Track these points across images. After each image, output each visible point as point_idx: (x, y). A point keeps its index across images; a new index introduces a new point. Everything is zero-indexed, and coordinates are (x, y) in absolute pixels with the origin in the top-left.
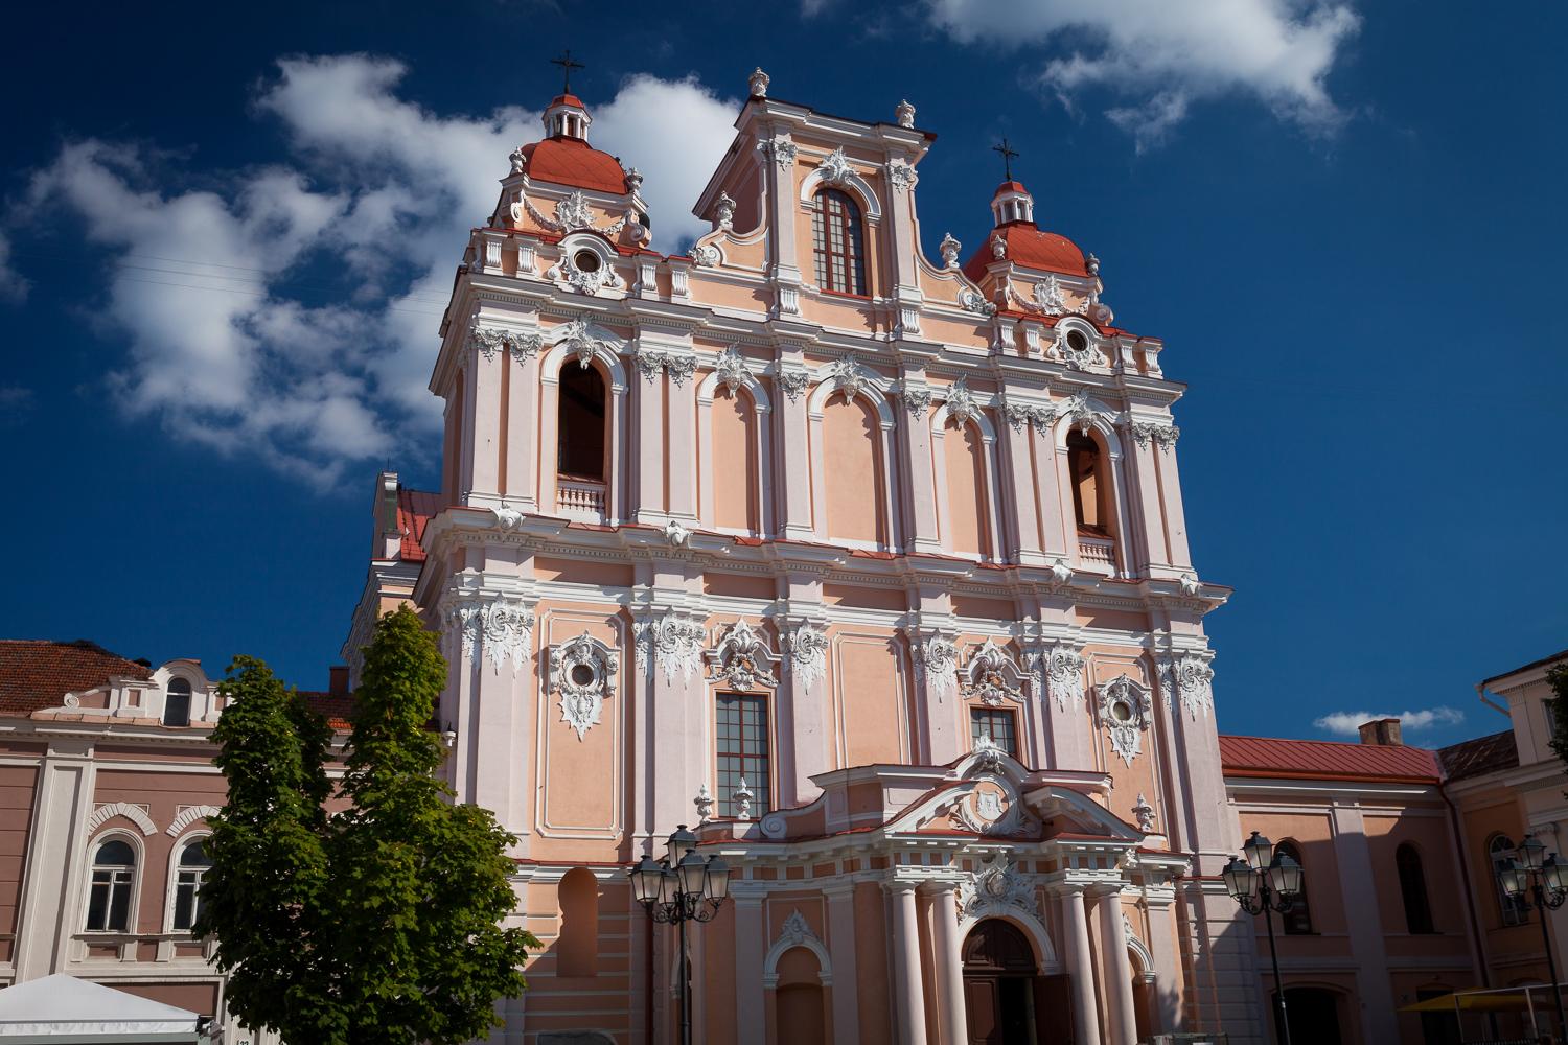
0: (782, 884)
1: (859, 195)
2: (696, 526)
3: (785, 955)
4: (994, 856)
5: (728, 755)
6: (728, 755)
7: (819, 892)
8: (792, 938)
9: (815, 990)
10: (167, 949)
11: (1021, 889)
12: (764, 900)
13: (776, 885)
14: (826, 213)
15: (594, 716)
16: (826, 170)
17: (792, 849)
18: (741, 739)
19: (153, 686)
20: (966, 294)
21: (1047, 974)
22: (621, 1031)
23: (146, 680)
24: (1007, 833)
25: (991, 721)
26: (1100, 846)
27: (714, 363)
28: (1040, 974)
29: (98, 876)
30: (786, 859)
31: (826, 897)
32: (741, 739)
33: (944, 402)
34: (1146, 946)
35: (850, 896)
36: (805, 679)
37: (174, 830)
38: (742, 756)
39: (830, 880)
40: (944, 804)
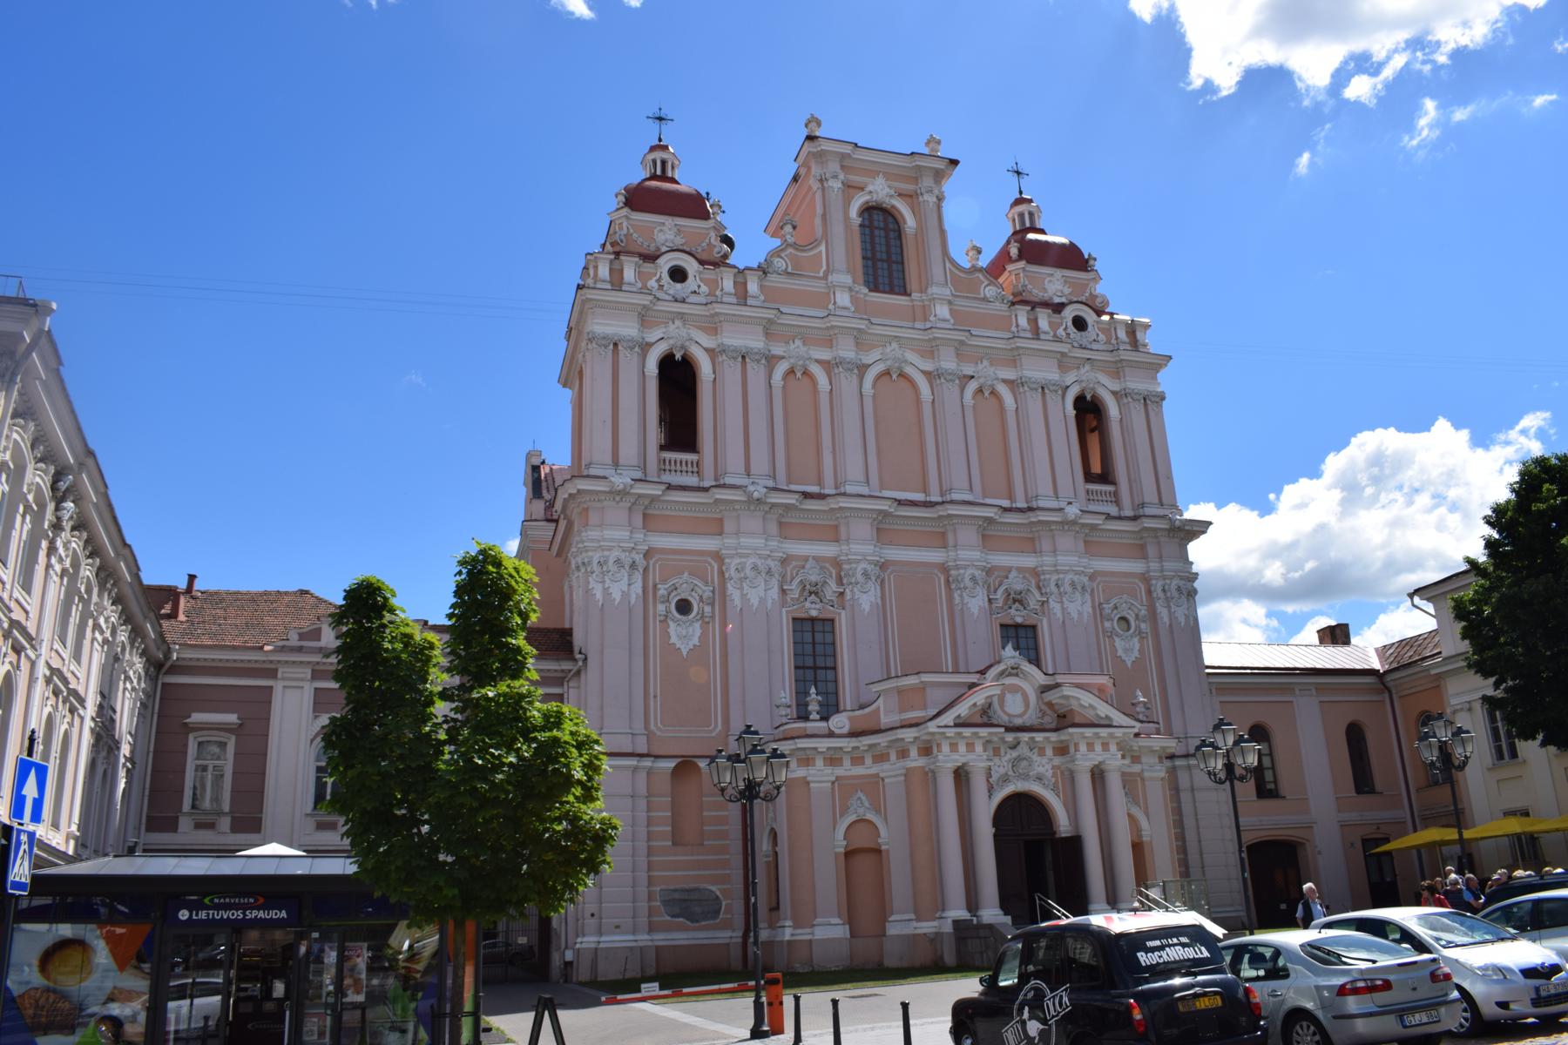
0: (847, 769)
1: (897, 210)
2: (771, 484)
3: (854, 823)
4: (1019, 743)
5: (804, 668)
6: (804, 668)
7: (877, 775)
11: (1041, 769)
12: (833, 783)
14: (871, 227)
15: (696, 641)
16: (871, 192)
17: (854, 742)
20: (987, 289)
21: (1063, 835)
22: (725, 887)
26: (1104, 732)
28: (1057, 836)
30: (850, 749)
31: (883, 779)
32: (814, 655)
33: (973, 377)
35: (903, 778)
38: (815, 668)
39: (886, 766)
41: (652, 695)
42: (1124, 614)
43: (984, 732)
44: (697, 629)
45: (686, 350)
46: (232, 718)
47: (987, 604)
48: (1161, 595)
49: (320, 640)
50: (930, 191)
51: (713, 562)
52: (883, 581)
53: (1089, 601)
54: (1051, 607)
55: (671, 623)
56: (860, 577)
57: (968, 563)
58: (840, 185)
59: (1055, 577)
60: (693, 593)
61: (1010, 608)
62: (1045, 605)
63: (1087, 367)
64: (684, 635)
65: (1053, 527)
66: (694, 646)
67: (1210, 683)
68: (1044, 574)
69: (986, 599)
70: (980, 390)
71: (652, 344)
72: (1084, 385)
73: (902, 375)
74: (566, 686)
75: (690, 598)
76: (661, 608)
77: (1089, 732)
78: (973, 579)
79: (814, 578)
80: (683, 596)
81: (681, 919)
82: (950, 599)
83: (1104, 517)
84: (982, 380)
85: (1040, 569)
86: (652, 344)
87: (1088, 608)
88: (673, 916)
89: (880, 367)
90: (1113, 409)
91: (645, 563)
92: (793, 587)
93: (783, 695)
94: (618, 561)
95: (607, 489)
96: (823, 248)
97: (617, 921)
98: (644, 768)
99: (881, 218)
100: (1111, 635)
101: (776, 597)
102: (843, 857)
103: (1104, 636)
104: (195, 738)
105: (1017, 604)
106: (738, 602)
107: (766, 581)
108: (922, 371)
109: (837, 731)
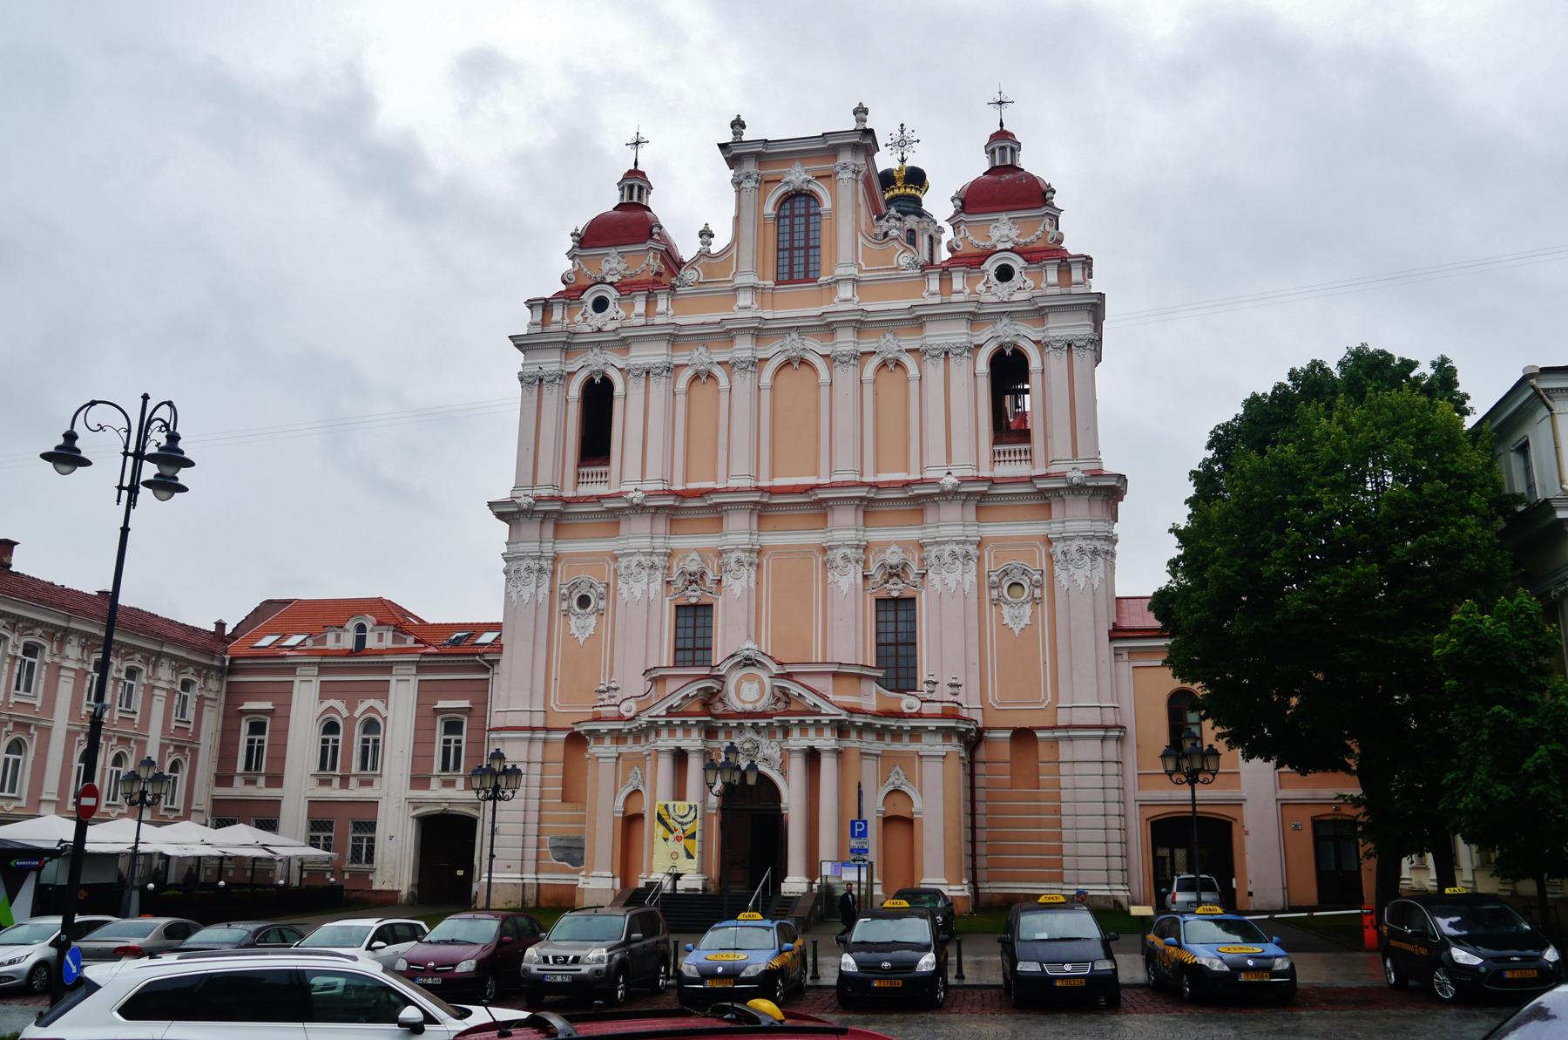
6: (685, 649)
9: (640, 817)
10: (353, 782)
15: (591, 631)
18: (694, 638)
19: (345, 631)
20: (903, 255)
23: (342, 627)
24: (760, 711)
26: (810, 719)
27: (689, 360)
29: (325, 741)
33: (875, 353)
37: (357, 714)
41: (553, 678)
43: (692, 721)
44: (593, 620)
45: (604, 373)
46: (268, 705)
47: (860, 580)
48: (1061, 557)
49: (325, 644)
50: (845, 167)
51: (610, 562)
52: (758, 566)
53: (974, 569)
55: (572, 617)
56: (733, 566)
57: (840, 543)
58: (753, 184)
59: (934, 551)
61: (887, 582)
63: (1006, 320)
64: (582, 626)
65: (936, 499)
67: (1115, 648)
68: (926, 546)
69: (861, 576)
70: (884, 364)
71: (574, 373)
72: (1000, 340)
73: (803, 362)
74: (491, 673)
76: (565, 605)
77: (794, 720)
78: (845, 557)
79: (693, 568)
80: (583, 593)
81: (565, 863)
82: (825, 577)
83: (988, 484)
84: (882, 355)
85: (920, 542)
86: (574, 373)
87: (971, 577)
88: (558, 860)
89: (781, 359)
90: (1035, 363)
91: (551, 567)
92: (674, 579)
94: (528, 568)
95: (516, 509)
96: (734, 251)
97: (509, 863)
98: (540, 739)
99: (803, 204)
100: (996, 603)
101: (659, 588)
102: (619, 824)
103: (991, 604)
104: (247, 720)
105: (895, 578)
106: (625, 595)
107: (649, 575)
108: (822, 356)
109: (626, 714)
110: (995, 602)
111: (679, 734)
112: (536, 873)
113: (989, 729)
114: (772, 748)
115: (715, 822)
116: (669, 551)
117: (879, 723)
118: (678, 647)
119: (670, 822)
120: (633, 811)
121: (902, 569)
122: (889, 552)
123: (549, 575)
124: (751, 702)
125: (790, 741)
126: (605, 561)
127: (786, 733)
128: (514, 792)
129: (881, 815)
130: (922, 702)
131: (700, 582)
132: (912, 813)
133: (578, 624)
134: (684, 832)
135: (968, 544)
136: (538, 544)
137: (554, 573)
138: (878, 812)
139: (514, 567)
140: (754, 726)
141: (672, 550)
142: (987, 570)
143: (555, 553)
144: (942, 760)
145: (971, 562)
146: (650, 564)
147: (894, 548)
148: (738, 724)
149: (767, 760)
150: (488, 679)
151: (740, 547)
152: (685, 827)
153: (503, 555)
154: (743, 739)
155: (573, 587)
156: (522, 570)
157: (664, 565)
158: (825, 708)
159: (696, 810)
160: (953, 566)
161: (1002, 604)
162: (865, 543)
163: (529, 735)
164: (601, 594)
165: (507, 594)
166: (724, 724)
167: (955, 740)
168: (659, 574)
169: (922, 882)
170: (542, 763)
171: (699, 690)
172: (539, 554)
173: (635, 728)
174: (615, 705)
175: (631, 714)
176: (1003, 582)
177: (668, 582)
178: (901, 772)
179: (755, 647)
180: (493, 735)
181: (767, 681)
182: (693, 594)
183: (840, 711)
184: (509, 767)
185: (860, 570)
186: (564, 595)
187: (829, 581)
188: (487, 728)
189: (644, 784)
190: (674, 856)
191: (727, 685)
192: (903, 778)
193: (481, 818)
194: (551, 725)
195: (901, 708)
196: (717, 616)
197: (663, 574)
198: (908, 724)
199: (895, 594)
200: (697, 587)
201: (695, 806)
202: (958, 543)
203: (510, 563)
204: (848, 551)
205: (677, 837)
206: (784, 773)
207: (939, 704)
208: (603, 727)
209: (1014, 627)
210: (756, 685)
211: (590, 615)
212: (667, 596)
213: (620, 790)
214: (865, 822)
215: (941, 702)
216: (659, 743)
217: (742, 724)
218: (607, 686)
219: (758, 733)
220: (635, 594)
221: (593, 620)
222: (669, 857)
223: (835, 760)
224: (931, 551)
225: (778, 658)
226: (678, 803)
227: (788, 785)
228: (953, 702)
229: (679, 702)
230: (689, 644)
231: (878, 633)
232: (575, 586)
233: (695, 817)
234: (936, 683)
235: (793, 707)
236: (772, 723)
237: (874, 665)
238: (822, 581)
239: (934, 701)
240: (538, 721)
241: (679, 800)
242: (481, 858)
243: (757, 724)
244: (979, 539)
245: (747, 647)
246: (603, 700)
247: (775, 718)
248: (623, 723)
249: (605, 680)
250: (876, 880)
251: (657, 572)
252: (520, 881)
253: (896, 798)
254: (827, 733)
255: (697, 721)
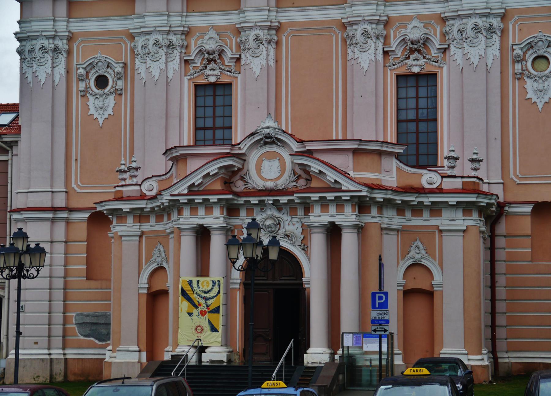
6: (205, 129)
8: (156, 261)
9: (165, 293)
13: (149, 227)
15: (110, 111)
18: (214, 117)
24: (281, 188)
25: (417, 83)
26: (330, 196)
30: (149, 210)
34: (437, 263)
36: (254, 69)
40: (209, 173)
42: (541, 53)
43: (213, 199)
44: (111, 100)
47: (380, 57)
51: (127, 41)
52: (278, 43)
54: (452, 53)
55: (88, 95)
56: (252, 43)
57: (360, 19)
59: (456, 25)
60: (109, 70)
61: (408, 58)
62: (447, 51)
66: (109, 115)
75: (106, 74)
76: (82, 86)
77: (315, 196)
78: (365, 33)
79: (211, 46)
80: (100, 72)
81: (91, 339)
82: (345, 54)
85: (442, 16)
87: (495, 51)
88: (85, 336)
91: (66, 47)
92: (192, 58)
93: (123, 162)
94: (42, 48)
98: (62, 219)
100: (520, 77)
101: (177, 67)
102: (144, 300)
105: (416, 54)
106: (143, 75)
107: (167, 54)
109: (149, 194)
110: (518, 76)
111: (201, 212)
112: (64, 348)
113: (510, 203)
114: (293, 224)
115: (239, 297)
116: (186, 29)
117: (399, 199)
118: (198, 126)
119: (194, 297)
120: (157, 287)
121: (424, 44)
122: (410, 26)
123: (65, 55)
124: (271, 180)
125: (311, 217)
126: (121, 40)
127: (308, 209)
128: (38, 271)
129: (402, 288)
130: (443, 177)
131: (219, 61)
132: (432, 286)
133: (96, 104)
134: (208, 306)
135: (492, 16)
136: (52, 23)
137: (69, 53)
138: (399, 285)
139: (28, 48)
140: (276, 203)
141: (189, 28)
142: (511, 42)
143: (69, 32)
144: (461, 234)
145: (495, 36)
146: (168, 43)
147: (415, 23)
148: (260, 201)
149: (288, 236)
150: (7, 161)
151: (259, 24)
152: (209, 302)
153: (16, 34)
154: (264, 215)
155: (91, 66)
156: (37, 50)
157: (181, 42)
158: (346, 185)
159: (219, 286)
160: (475, 40)
161: (525, 78)
162: (385, 18)
163: (51, 215)
164: (119, 74)
165: (22, 75)
166: (245, 201)
167: (475, 215)
168: (176, 53)
169: (441, 352)
170: (66, 242)
171: (220, 168)
172: (53, 33)
173: (157, 206)
174: (136, 185)
175: (153, 193)
176: (527, 55)
177: (186, 61)
178: (421, 246)
179: (275, 125)
180: (15, 216)
181: (288, 159)
182: (211, 72)
183: (360, 188)
184: (33, 246)
185: (380, 45)
186: (81, 75)
187: (349, 58)
188: (9, 209)
189: (167, 261)
190: (199, 329)
191: (248, 164)
192: (423, 252)
193: (6, 297)
194: (74, 204)
195: (421, 185)
196: (236, 95)
197: (181, 52)
198: (428, 200)
199: (416, 70)
200: (216, 66)
201: (219, 281)
202: (481, 16)
203: (24, 43)
204: (369, 27)
205: (201, 311)
206: (305, 249)
207: (459, 180)
208: (126, 206)
209: (538, 101)
210: (276, 164)
211: (108, 95)
212: (185, 76)
213: (144, 268)
214: (386, 294)
215: (462, 177)
216: (182, 221)
217: (264, 201)
218: (128, 165)
219: (280, 210)
220: (153, 73)
221: (111, 100)
222: (194, 331)
223: (356, 234)
224: (453, 25)
225: (298, 136)
226: (202, 279)
227: (309, 260)
228: (474, 177)
229: (201, 180)
230: (209, 123)
231: (398, 110)
232: (92, 66)
233: (219, 292)
234: (457, 159)
235: (314, 184)
236: (293, 200)
237: (394, 141)
238: (342, 58)
239: (455, 177)
240: (60, 201)
241: (202, 275)
242: (7, 335)
243: (278, 201)
244: (503, 11)
245: (265, 125)
246: (125, 180)
247: (296, 195)
248: (145, 202)
249: (125, 160)
250: (396, 351)
251: (175, 51)
252: (47, 357)
253: (417, 272)
254: (348, 209)
255: (219, 200)
